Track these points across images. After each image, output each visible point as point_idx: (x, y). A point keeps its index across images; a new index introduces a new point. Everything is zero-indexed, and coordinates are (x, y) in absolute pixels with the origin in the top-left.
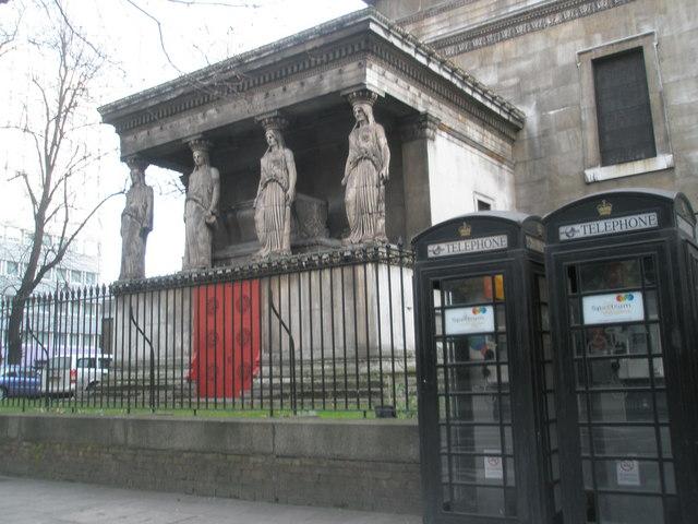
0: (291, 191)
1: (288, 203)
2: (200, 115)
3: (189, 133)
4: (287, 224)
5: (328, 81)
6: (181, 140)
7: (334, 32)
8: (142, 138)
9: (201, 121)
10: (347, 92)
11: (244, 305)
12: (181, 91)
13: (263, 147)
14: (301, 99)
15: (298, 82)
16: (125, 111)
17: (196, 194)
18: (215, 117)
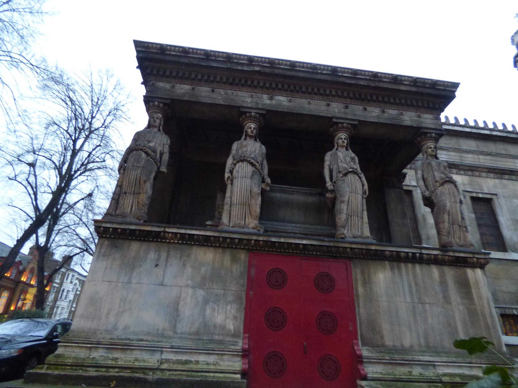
0: (366, 187)
1: (365, 197)
2: (265, 96)
3: (249, 105)
4: (365, 213)
5: (409, 118)
6: (239, 107)
7: (426, 87)
8: (183, 89)
9: (268, 102)
10: (428, 131)
11: (325, 284)
12: (257, 69)
13: (329, 145)
14: (382, 121)
15: (378, 109)
16: (176, 59)
17: (253, 158)
18: (285, 103)
